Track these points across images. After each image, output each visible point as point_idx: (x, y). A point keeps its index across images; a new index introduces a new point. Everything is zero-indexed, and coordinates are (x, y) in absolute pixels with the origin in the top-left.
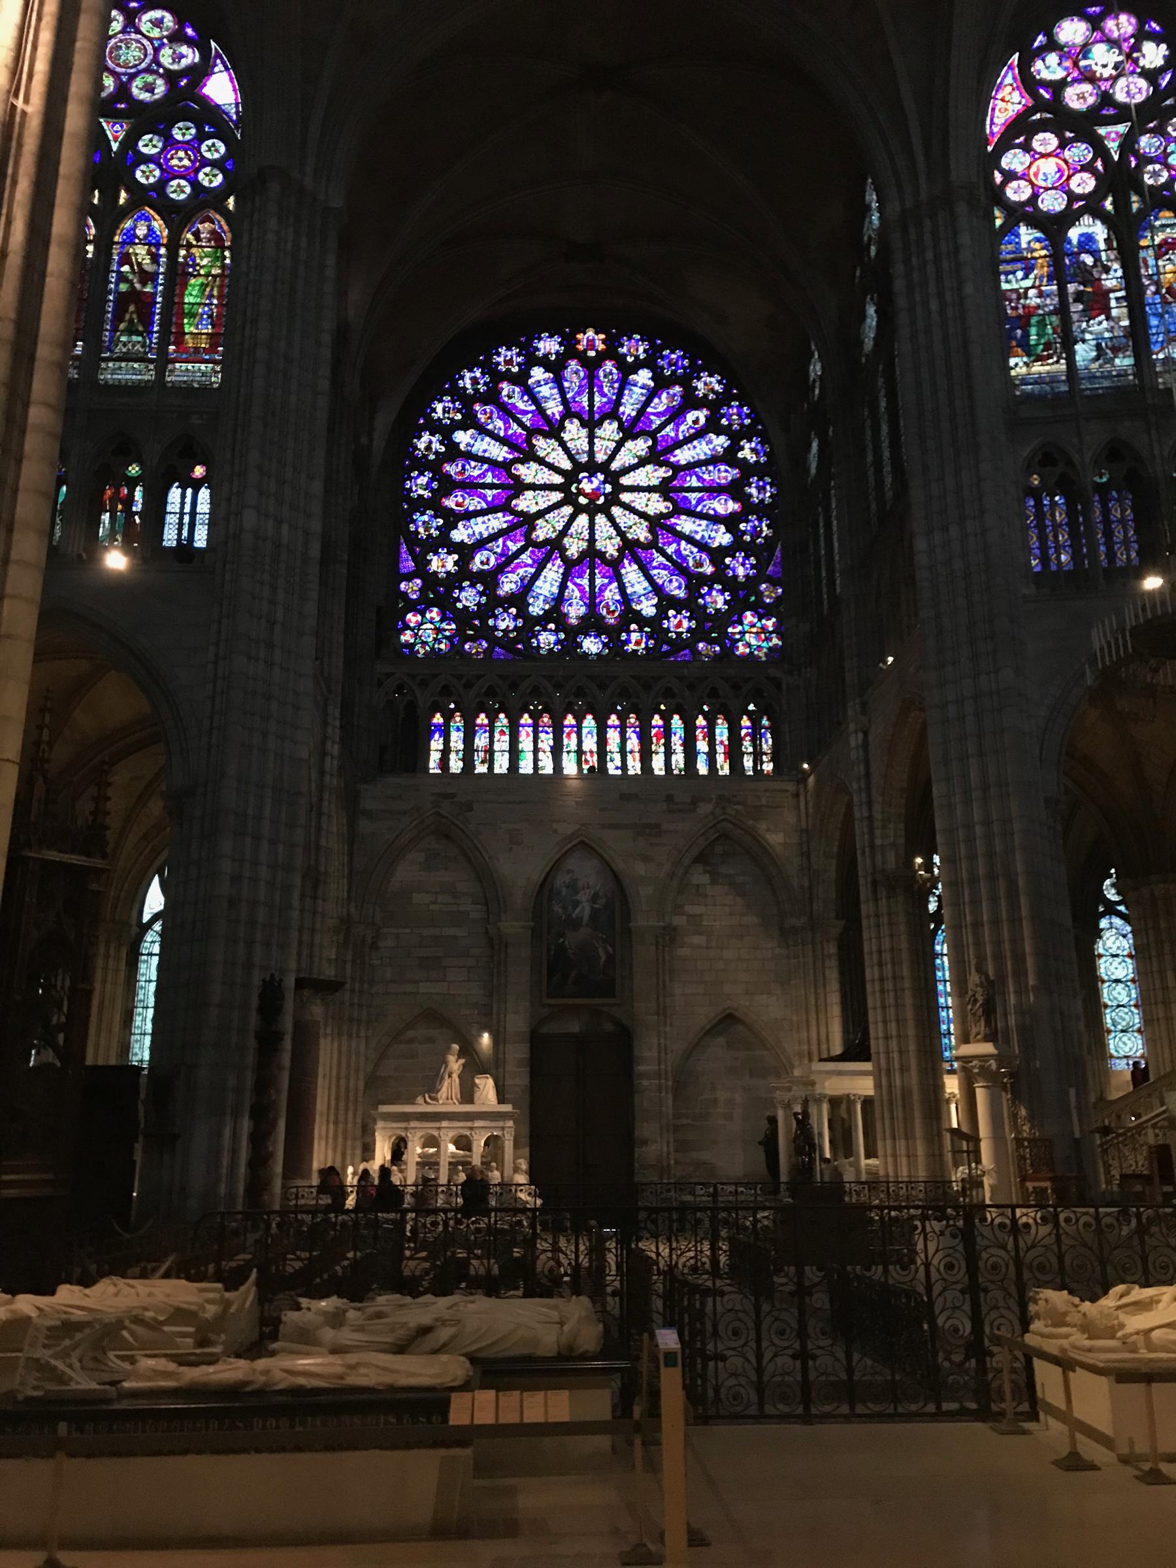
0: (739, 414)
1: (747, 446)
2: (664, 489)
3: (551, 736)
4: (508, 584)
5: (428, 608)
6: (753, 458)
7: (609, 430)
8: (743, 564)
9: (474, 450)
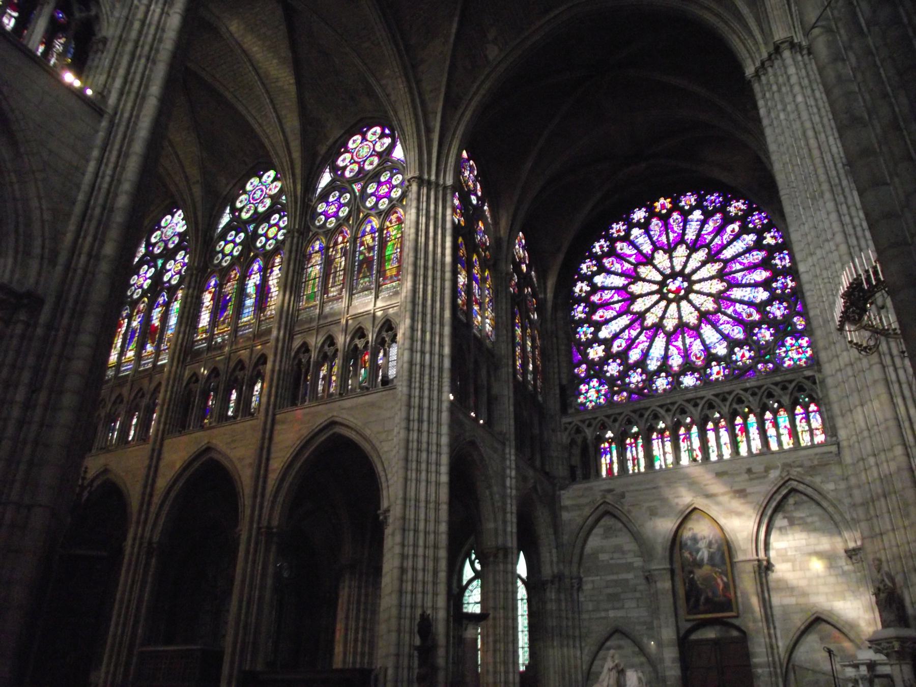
0: (759, 219)
2: (721, 275)
4: (634, 355)
5: (591, 380)
6: (773, 242)
8: (779, 308)
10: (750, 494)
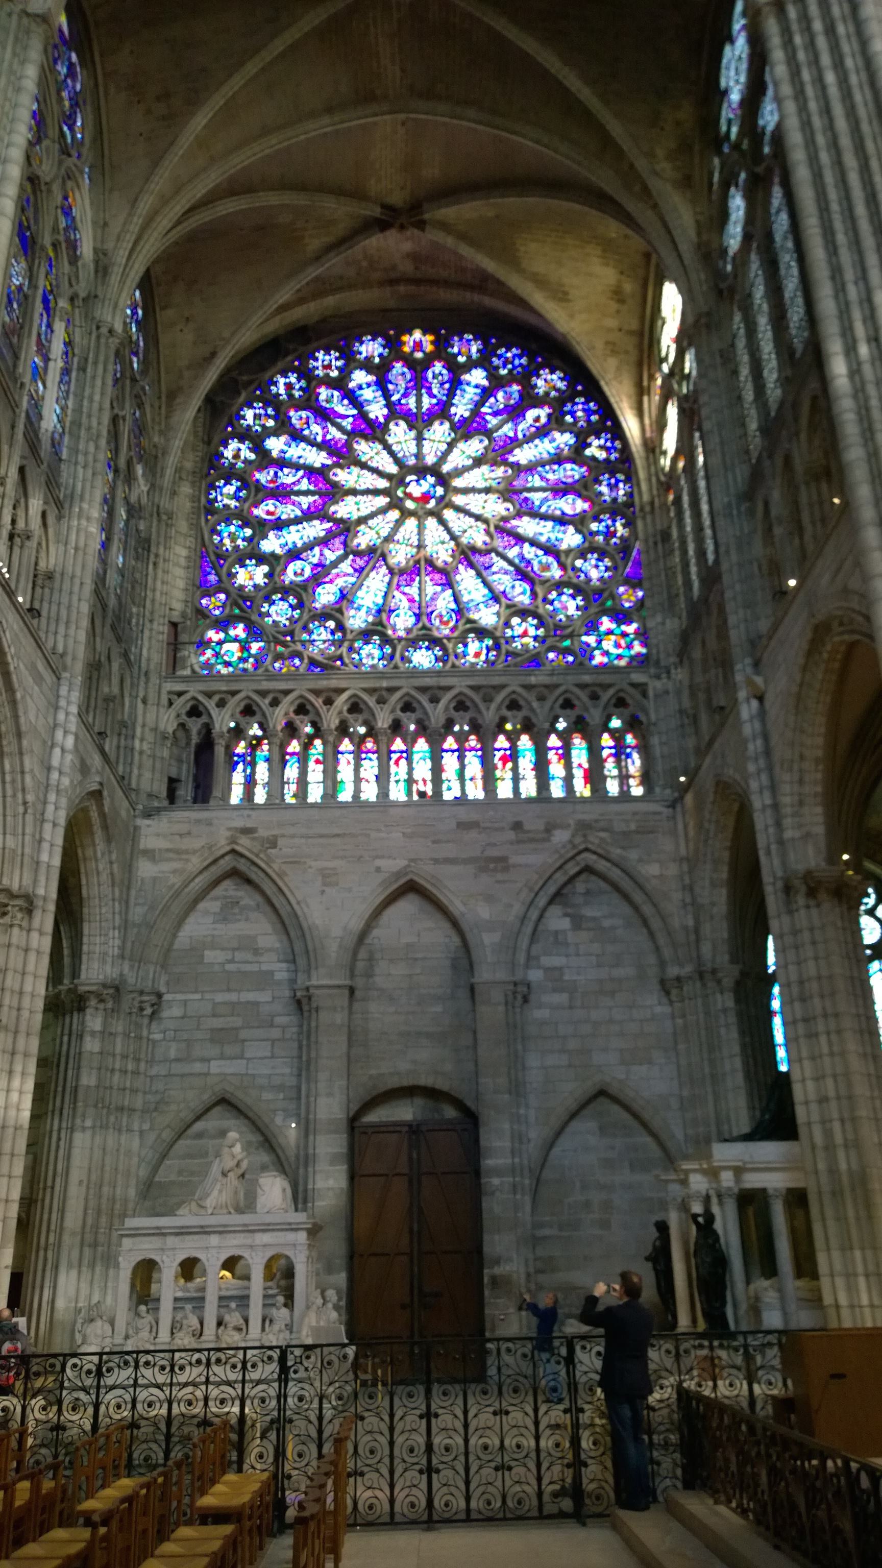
1: (596, 443)
3: (376, 763)
6: (602, 455)
8: (597, 566)
9: (287, 456)
10: (514, 866)
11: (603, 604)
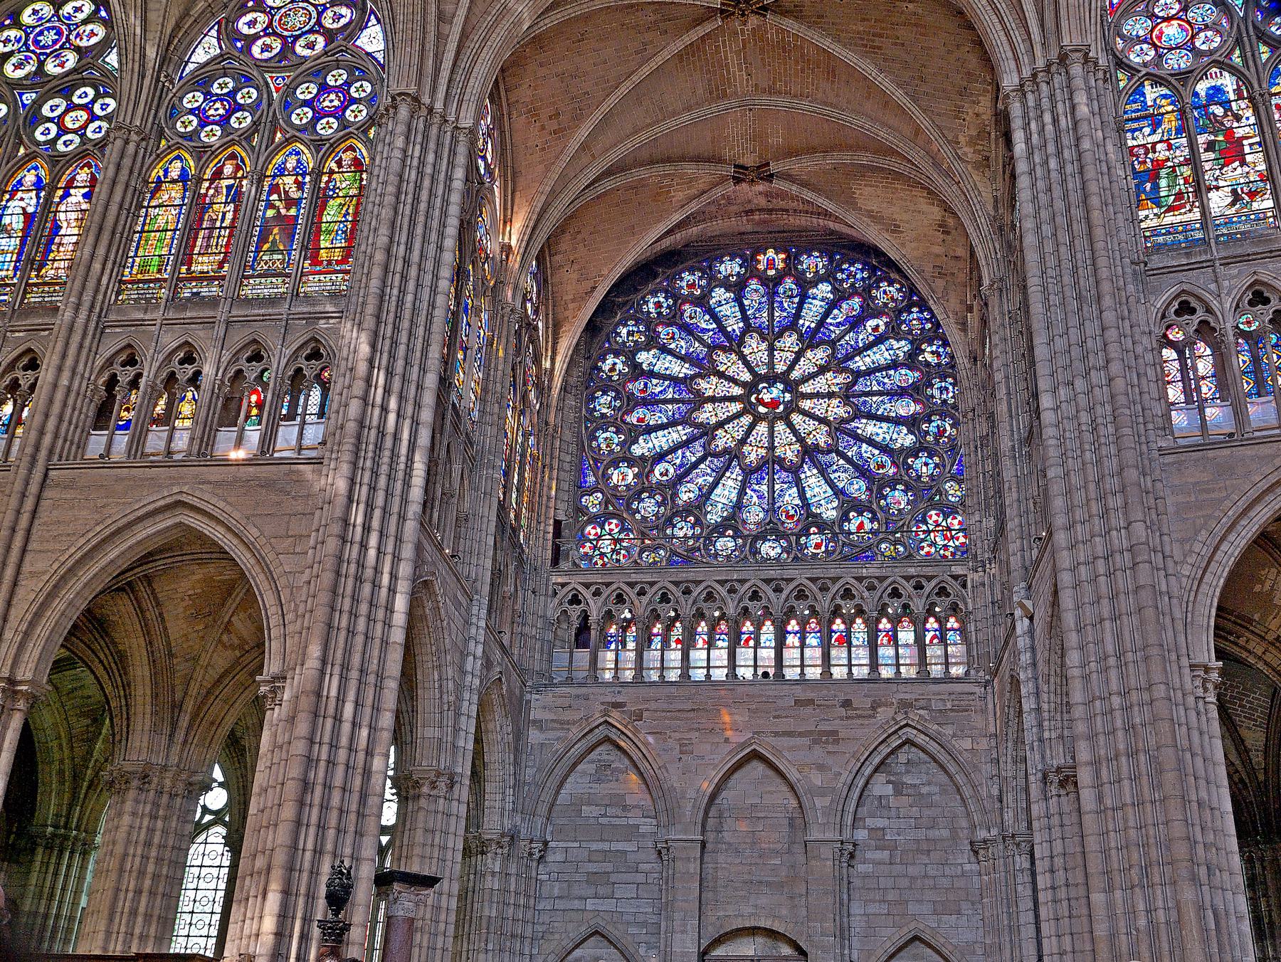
0: (919, 319)
2: (846, 395)
7: (789, 341)
8: (926, 464)
9: (656, 369)
11: (931, 499)
